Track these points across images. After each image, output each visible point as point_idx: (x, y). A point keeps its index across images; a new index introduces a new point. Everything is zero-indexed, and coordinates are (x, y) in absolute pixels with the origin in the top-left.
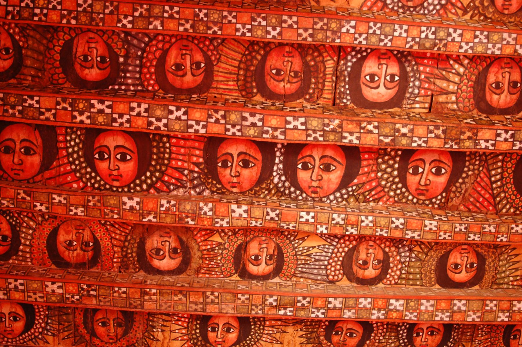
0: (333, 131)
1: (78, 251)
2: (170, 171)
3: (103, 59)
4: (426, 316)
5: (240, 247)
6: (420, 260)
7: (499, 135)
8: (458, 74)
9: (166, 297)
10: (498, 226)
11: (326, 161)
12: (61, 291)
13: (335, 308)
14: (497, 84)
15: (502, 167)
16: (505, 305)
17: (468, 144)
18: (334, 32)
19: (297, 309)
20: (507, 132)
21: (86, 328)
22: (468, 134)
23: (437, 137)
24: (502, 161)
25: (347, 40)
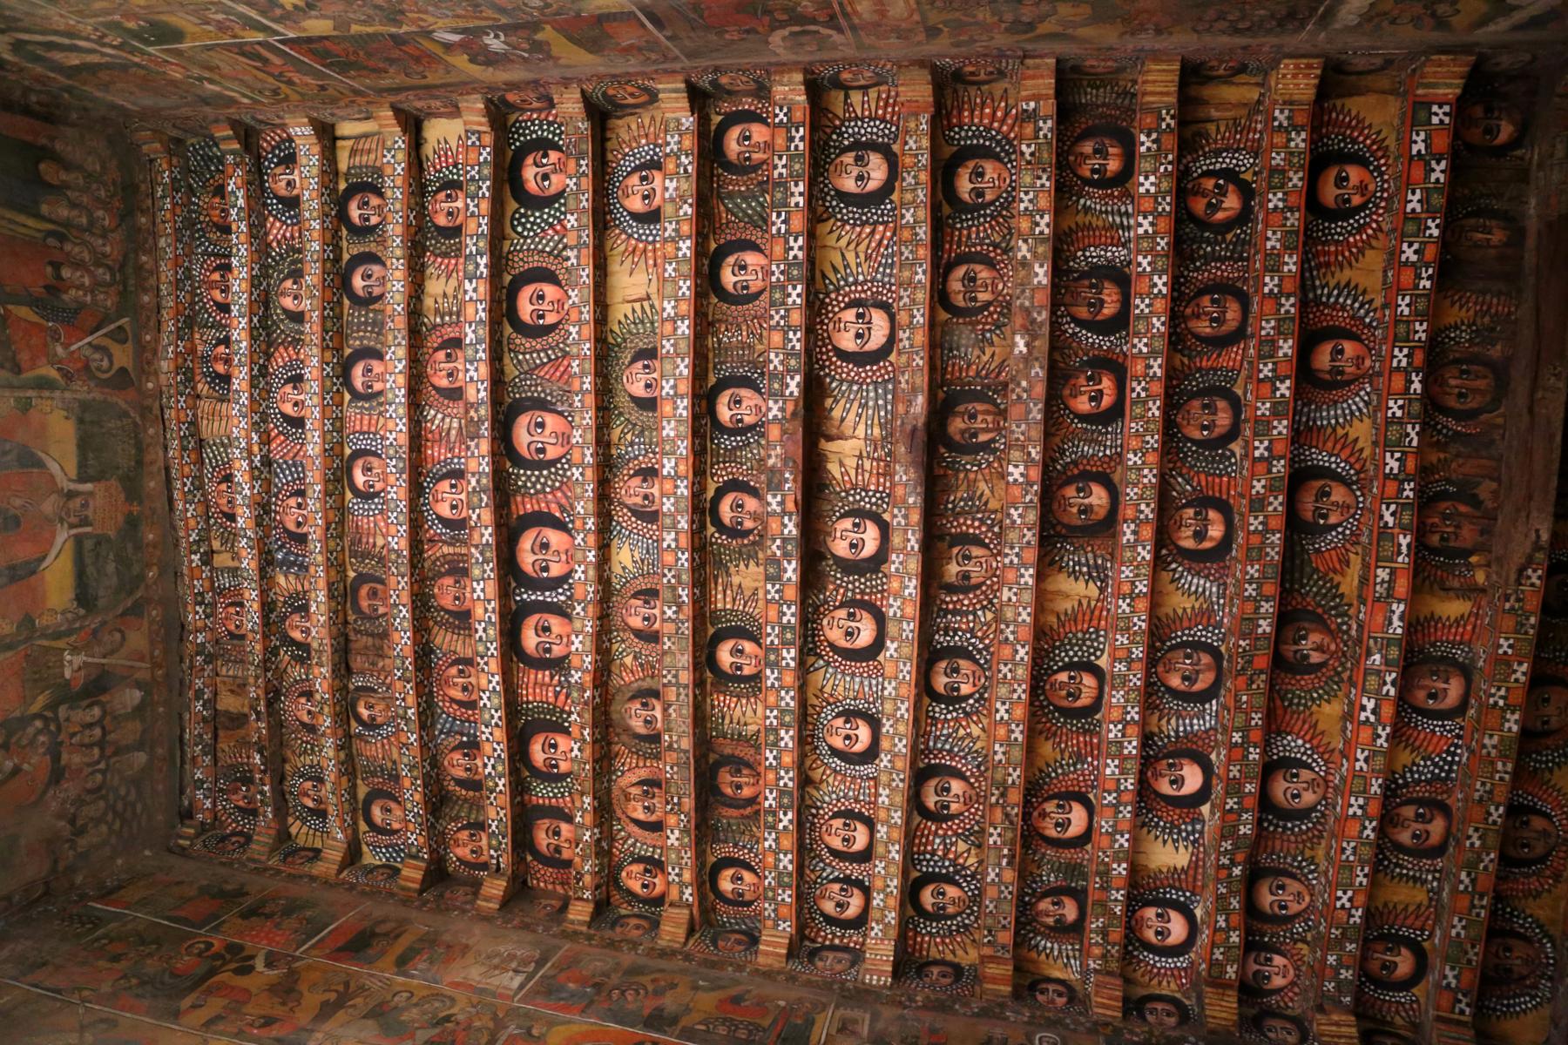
0: (482, 553)
3: (465, 755)
5: (637, 636)
6: (642, 432)
9: (673, 725)
10: (573, 358)
11: (537, 549)
12: (677, 832)
13: (676, 540)
14: (450, 375)
16: (668, 327)
17: (482, 412)
19: (680, 583)
20: (467, 371)
21: (744, 807)
22: (472, 413)
23: (477, 446)
25: (404, 544)
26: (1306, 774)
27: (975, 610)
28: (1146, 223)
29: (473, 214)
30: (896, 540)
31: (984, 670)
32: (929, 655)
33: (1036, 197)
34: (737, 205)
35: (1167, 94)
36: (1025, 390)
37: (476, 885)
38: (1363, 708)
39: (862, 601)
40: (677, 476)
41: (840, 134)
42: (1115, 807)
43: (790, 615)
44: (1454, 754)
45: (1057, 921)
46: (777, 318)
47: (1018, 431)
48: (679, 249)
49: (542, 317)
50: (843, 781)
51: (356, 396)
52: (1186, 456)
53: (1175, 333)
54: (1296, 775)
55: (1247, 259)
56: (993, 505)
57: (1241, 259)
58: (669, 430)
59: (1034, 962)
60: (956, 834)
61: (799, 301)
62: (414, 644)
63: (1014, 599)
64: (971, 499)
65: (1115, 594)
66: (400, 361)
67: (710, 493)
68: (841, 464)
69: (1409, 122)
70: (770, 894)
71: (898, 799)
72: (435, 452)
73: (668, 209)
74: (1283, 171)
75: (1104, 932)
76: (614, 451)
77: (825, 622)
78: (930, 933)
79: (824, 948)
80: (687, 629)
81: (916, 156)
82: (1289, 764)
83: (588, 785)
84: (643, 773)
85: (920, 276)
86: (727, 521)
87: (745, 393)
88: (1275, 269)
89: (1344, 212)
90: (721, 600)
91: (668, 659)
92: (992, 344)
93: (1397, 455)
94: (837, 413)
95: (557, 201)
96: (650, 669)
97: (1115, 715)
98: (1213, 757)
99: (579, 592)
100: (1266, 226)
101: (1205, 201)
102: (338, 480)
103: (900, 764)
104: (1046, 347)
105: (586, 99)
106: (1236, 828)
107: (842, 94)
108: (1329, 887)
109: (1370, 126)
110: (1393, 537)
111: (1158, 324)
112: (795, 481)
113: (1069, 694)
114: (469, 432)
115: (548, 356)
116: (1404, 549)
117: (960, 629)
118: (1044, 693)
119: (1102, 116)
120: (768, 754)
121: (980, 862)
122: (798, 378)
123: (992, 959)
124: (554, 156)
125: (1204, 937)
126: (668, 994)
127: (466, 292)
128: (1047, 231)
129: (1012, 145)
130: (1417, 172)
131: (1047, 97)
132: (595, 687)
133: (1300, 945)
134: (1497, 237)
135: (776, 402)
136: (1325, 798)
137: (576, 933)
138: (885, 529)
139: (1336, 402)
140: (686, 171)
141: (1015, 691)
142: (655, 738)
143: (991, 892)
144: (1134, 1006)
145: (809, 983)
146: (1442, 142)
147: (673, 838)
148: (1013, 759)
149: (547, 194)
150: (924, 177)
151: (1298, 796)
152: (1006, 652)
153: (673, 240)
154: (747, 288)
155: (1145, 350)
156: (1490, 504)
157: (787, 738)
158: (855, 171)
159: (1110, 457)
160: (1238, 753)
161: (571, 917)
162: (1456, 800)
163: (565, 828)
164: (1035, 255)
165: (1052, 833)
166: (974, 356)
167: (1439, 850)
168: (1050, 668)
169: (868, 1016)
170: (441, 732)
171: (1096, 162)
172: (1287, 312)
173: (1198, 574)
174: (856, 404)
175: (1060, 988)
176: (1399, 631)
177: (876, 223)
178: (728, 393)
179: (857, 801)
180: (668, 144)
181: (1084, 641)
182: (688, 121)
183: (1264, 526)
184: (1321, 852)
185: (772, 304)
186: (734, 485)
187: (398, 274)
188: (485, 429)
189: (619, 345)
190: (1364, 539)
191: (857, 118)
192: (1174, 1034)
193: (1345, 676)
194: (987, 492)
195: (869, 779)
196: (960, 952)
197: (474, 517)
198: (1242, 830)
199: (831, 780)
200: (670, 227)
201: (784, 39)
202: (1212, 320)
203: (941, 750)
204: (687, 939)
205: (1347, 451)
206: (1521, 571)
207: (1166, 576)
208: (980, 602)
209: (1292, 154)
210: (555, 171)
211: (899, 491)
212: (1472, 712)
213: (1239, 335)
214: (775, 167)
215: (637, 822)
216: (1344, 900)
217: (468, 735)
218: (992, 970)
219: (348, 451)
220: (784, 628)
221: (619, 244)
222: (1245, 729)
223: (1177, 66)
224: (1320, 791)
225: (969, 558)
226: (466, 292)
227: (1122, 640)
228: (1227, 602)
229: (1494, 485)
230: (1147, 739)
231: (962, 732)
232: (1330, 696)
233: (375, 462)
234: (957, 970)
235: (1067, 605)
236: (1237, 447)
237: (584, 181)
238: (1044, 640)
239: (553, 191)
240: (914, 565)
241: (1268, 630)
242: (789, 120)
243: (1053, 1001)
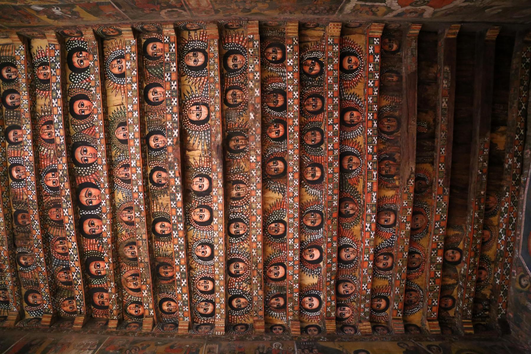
0: (66, 199)
1: (137, 281)
2: (100, 250)
3: (65, 273)
4: (137, 150)
5: (126, 224)
7: (57, 135)
8: (47, 151)
11: (87, 196)
12: (146, 291)
13: (138, 189)
14: (49, 134)
15: (80, 125)
16: (130, 114)
17: (63, 147)
18: (33, 202)
19: (140, 204)
20: (56, 132)
21: (169, 280)
22: (59, 148)
23: (61, 160)
24: (77, 125)
25: (34, 197)
26: (351, 249)
28: (290, 75)
29: (54, 75)
30: (214, 184)
31: (247, 225)
32: (228, 222)
33: (254, 67)
34: (152, 71)
35: (295, 33)
36: (254, 131)
37: (73, 319)
38: (366, 227)
39: (204, 205)
40: (137, 166)
41: (188, 46)
42: (293, 266)
43: (180, 212)
44: (393, 238)
45: (277, 306)
46: (169, 110)
47: (253, 145)
48: (132, 87)
49: (83, 112)
50: (203, 267)
51: (11, 143)
52: (307, 150)
53: (302, 110)
54: (348, 250)
55: (323, 86)
56: (246, 170)
57: (321, 86)
58: (133, 151)
59: (271, 320)
60: (242, 281)
61: (176, 104)
62: (42, 234)
64: (239, 168)
65: (288, 197)
66: (28, 130)
67: (149, 172)
68: (194, 159)
69: (368, 43)
70: (181, 309)
71: (222, 271)
72: (46, 163)
73: (128, 73)
74: (332, 58)
75: (293, 307)
76: (113, 159)
77: (192, 213)
78: (236, 315)
79: (201, 325)
80: (144, 220)
81: (214, 53)
82: (346, 247)
83: (112, 278)
84: (132, 272)
85: (217, 94)
86: (156, 181)
87: (159, 136)
88: (331, 89)
89: (351, 71)
90: (155, 209)
91: (138, 231)
92: (242, 116)
93: (371, 147)
94: (191, 142)
95: (87, 70)
96: (132, 235)
97: (291, 236)
98: (323, 247)
99: (104, 210)
100: (328, 75)
101: (309, 67)
102: (6, 175)
103: (221, 259)
104: (260, 117)
105: (95, 33)
107: (187, 32)
108: (360, 284)
109: (357, 44)
110: (371, 173)
111: (296, 108)
112: (178, 166)
113: (276, 231)
114: (58, 155)
115: (87, 126)
116: (375, 176)
118: (267, 231)
119: (274, 40)
120: (176, 260)
121: (251, 289)
122: (177, 130)
123: (257, 321)
124: (84, 54)
125: (324, 304)
126: (147, 349)
127: (53, 104)
128: (258, 78)
129: (246, 50)
130: (371, 59)
131: (256, 34)
132: (112, 243)
133: (353, 303)
134: (395, 78)
135: (170, 139)
136: (357, 256)
137: (112, 332)
138: (210, 180)
139: (352, 131)
140: (133, 59)
142: (136, 259)
143: (255, 299)
144: (304, 330)
145: (197, 338)
146: (378, 49)
147: (145, 294)
148: (259, 254)
149: (82, 67)
150: (217, 60)
151: (349, 256)
152: (254, 218)
153: (130, 83)
154: (158, 100)
155: (292, 116)
156: (398, 160)
157: (182, 254)
158: (193, 59)
159: (283, 152)
160: (330, 245)
161: (110, 326)
162: (394, 252)
163: (105, 295)
164: (255, 86)
165: (273, 277)
166: (237, 120)
167: (391, 268)
168: (269, 222)
169: (217, 346)
170: (55, 265)
171: (273, 55)
172: (336, 103)
173: (314, 188)
174: (198, 138)
175: (280, 327)
176: (375, 202)
177: (201, 76)
178: (153, 136)
179: (208, 273)
180: (127, 49)
181: (279, 213)
182: (133, 41)
183: (333, 171)
184: (357, 273)
185: (167, 105)
186: (158, 169)
187: (25, 97)
188: (64, 153)
189: (113, 121)
190: (363, 174)
191: (193, 41)
192: (317, 337)
193: (361, 217)
194: (244, 166)
195: (212, 265)
196: (247, 320)
197: (62, 186)
198: (333, 269)
199: (198, 267)
200: (129, 79)
201: (165, 13)
202: (313, 106)
203: (235, 253)
204: (153, 328)
205: (356, 146)
206: (408, 180)
207: (304, 190)
208: (244, 202)
209: (334, 52)
210: (85, 59)
211: (214, 167)
212: (397, 225)
213: (322, 110)
214: (165, 57)
215: (131, 289)
216: (365, 287)
217: (65, 265)
218: (258, 324)
219: (9, 164)
220: (178, 217)
221: (110, 85)
222: (332, 237)
223: (297, 24)
224: (356, 254)
225: (239, 188)
226: (53, 104)
227: (291, 211)
228: (324, 197)
229: (399, 155)
230: (301, 243)
231: (241, 247)
232: (356, 224)
233: (21, 168)
234: (247, 326)
235: (272, 202)
236: (323, 146)
237: (96, 63)
238: (266, 213)
239: (85, 66)
240: (221, 192)
241: (336, 204)
242: (169, 41)
243: (278, 332)
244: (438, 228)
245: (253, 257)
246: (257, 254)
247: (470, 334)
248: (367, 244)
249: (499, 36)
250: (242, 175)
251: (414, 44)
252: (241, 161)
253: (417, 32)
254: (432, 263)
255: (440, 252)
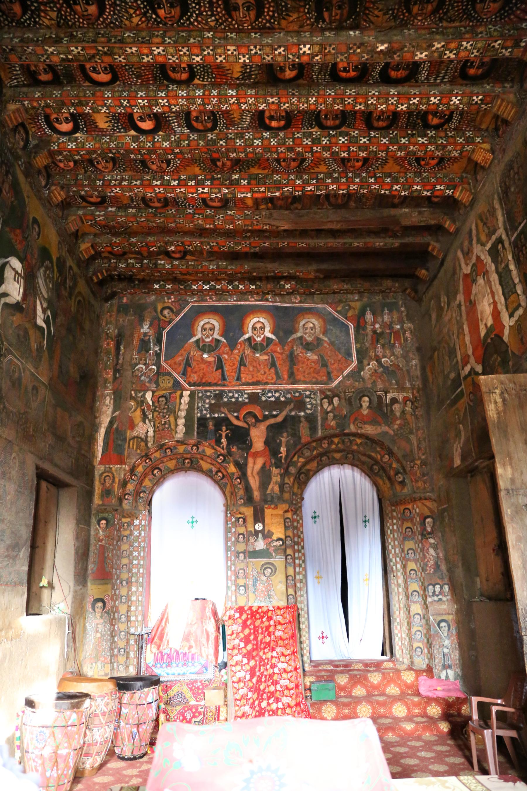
27: (215, 16)
35: (498, 110)
38: (203, 189)
42: (121, 105)
45: (34, 71)
54: (162, 162)
57: (406, 128)
63: (229, 53)
75: (48, 106)
106: (132, 153)
108: (119, 184)
110: (278, 191)
117: (200, 7)
130: (428, 188)
141: (173, 57)
143: (39, 50)
148: (130, 58)
151: (153, 163)
156: (292, 207)
192: (20, 152)
194: (292, 19)
198: (132, 156)
208: (220, 18)
225: (248, 10)
231: (132, 11)
244: (209, 245)
245: (121, 48)
246: (129, 55)
247: (93, 280)
248: (178, 190)
249: (418, 278)
250: (272, 17)
251: (433, 222)
252: (301, 14)
253: (446, 226)
254: (166, 243)
255: (181, 248)
